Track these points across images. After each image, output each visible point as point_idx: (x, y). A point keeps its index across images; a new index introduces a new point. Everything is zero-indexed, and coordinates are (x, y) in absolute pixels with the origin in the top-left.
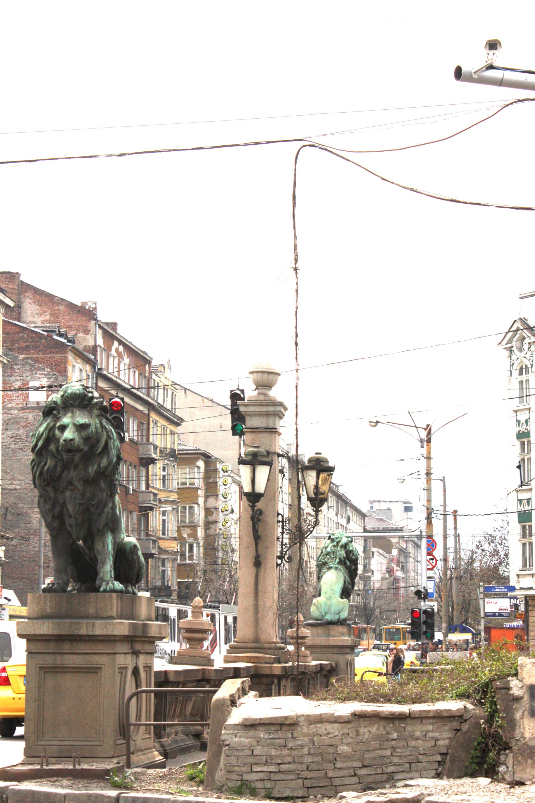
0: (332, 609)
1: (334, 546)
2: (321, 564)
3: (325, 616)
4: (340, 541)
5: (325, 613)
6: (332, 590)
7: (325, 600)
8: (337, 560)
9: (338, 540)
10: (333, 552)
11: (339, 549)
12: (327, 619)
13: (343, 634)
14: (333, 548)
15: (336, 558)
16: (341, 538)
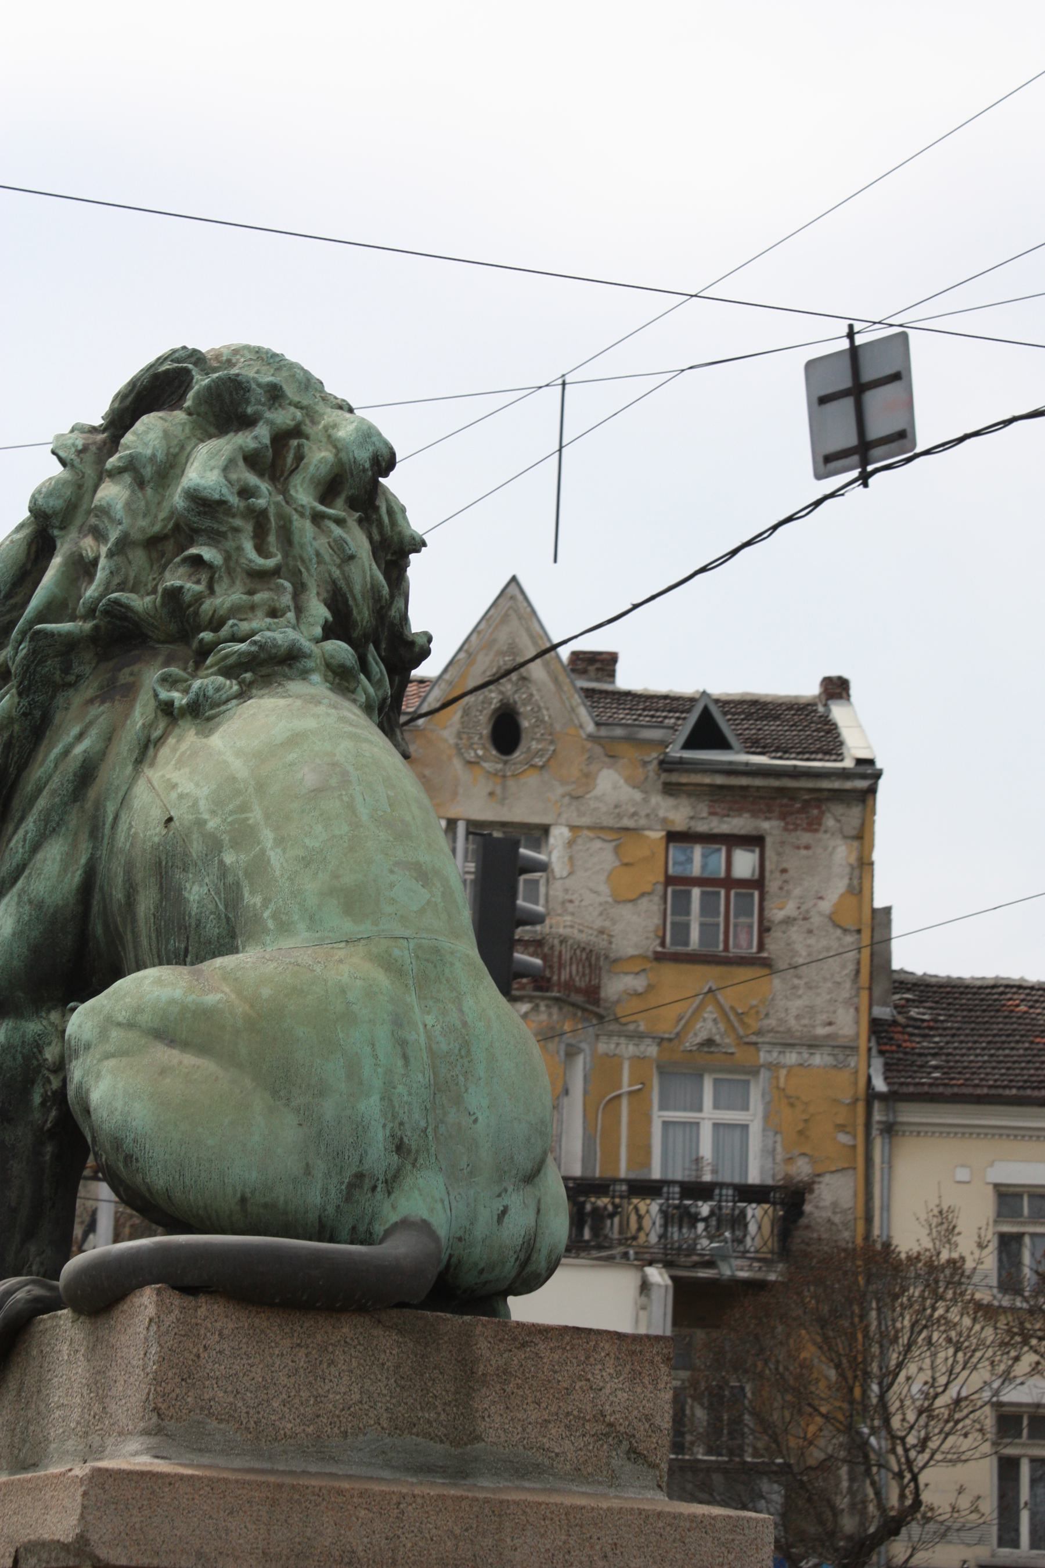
0: (476, 1099)
1: (252, 460)
2: (70, 645)
3: (392, 1182)
4: (296, 432)
5: (400, 1148)
6: (423, 875)
7: (382, 979)
8: (319, 611)
9: (284, 417)
10: (260, 520)
11: (304, 495)
12: (425, 1227)
13: (634, 1454)
14: (252, 479)
15: (299, 589)
16: (310, 413)
